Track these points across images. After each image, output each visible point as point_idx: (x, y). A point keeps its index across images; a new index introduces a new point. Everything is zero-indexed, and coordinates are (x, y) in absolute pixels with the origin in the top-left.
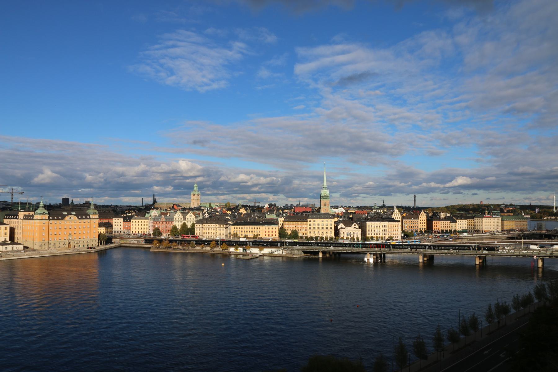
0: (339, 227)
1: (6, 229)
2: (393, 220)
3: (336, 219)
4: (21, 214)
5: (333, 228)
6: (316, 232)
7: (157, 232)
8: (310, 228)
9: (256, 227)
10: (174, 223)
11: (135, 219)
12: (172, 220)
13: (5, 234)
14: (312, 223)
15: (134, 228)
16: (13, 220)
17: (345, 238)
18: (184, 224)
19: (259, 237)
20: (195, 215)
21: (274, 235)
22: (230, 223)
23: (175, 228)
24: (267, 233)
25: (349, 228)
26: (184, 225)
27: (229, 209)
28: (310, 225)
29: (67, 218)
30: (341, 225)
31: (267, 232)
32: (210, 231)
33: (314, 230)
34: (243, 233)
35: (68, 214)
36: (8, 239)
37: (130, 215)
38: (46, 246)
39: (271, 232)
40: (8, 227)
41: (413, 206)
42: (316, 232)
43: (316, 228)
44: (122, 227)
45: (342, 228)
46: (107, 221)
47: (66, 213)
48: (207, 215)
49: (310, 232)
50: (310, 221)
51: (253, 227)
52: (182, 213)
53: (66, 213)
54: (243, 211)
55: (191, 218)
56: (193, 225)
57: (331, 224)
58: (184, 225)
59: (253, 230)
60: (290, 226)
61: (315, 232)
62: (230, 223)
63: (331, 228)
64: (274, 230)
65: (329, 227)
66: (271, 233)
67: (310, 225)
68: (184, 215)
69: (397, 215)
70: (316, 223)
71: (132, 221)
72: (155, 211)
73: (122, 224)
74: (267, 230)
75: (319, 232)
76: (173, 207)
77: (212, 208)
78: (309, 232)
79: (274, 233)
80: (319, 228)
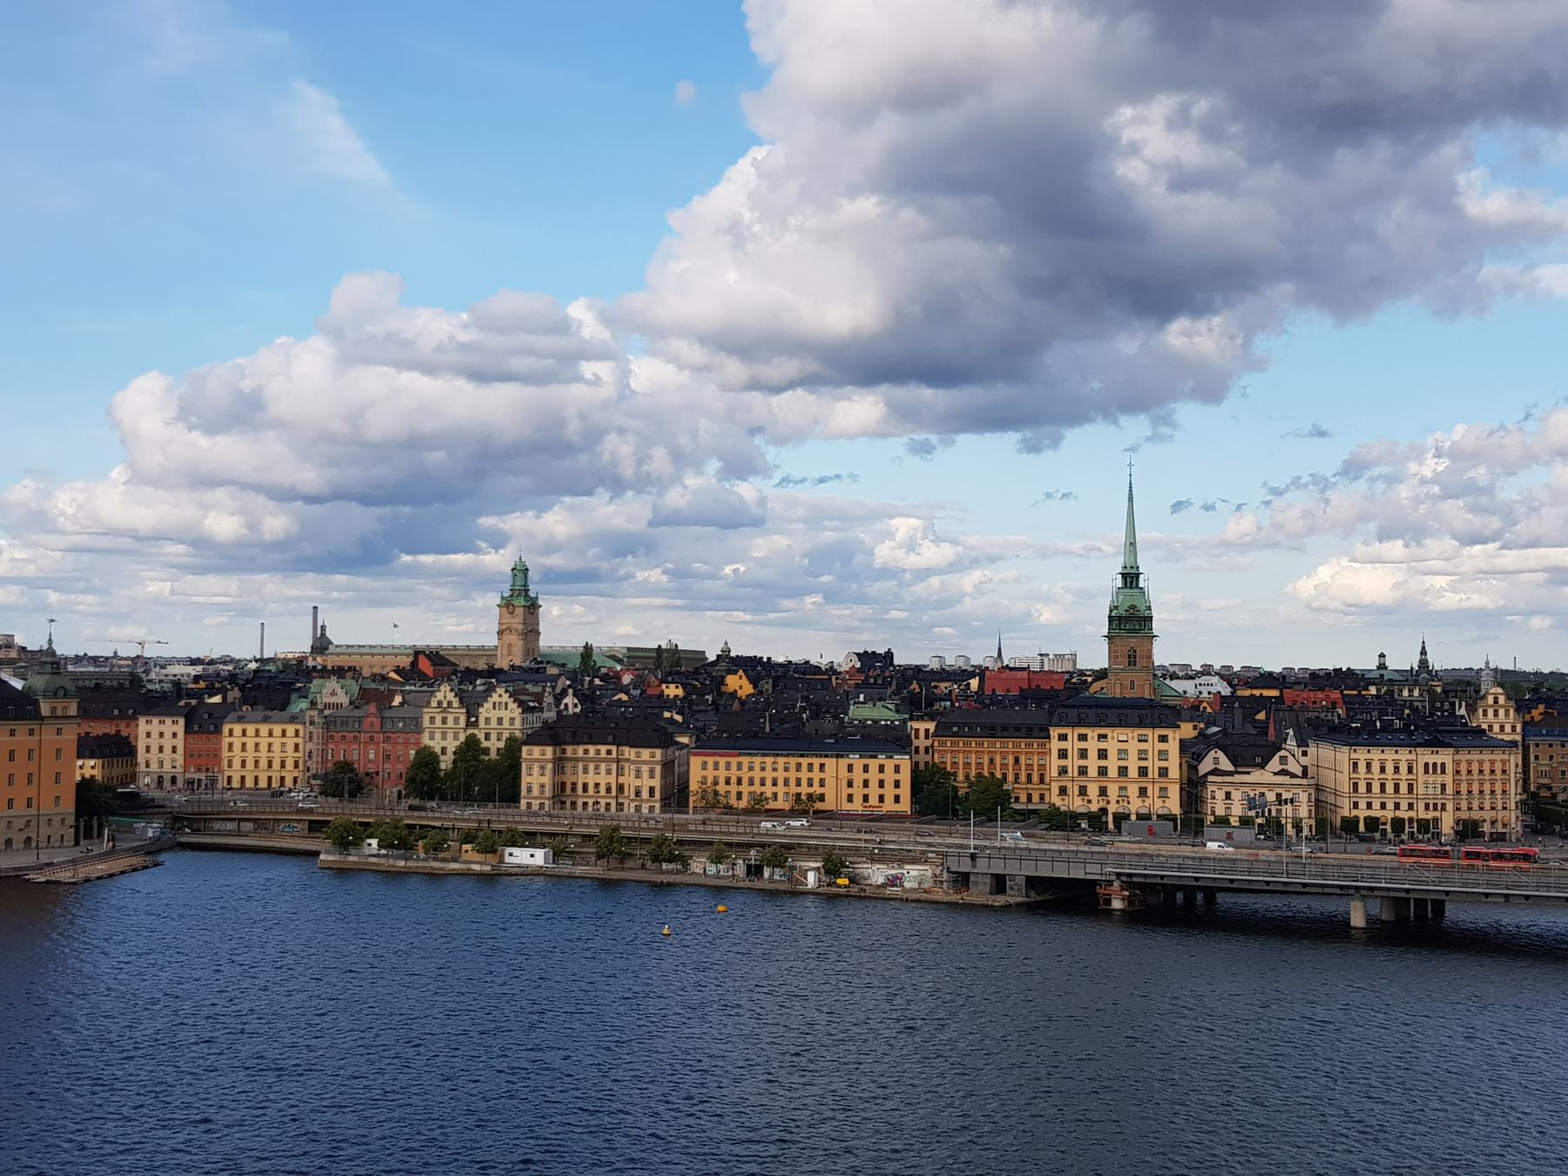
0: (1205, 766)
2: (1477, 738)
3: (1187, 730)
5: (1174, 773)
6: (1093, 791)
7: (343, 781)
8: (1063, 771)
9: (805, 761)
10: (426, 740)
11: (240, 720)
12: (415, 726)
14: (1073, 745)
15: (237, 764)
17: (1234, 821)
19: (819, 806)
20: (521, 704)
21: (889, 799)
22: (684, 740)
23: (427, 760)
24: (858, 792)
25: (1256, 776)
27: (670, 677)
28: (1063, 754)
30: (1217, 759)
31: (858, 782)
32: (591, 779)
33: (1082, 781)
34: (745, 788)
37: (217, 699)
39: (874, 784)
42: (1093, 791)
43: (1093, 772)
50: (1063, 737)
51: (793, 761)
52: (462, 696)
54: (738, 684)
55: (501, 716)
56: (512, 750)
57: (1163, 755)
58: (471, 748)
59: (792, 775)
60: (967, 759)
61: (1083, 791)
62: (684, 740)
63: (1163, 772)
65: (1153, 765)
66: (874, 792)
68: (471, 705)
69: (1499, 719)
70: (1093, 746)
71: (226, 728)
72: (332, 683)
73: (180, 742)
74: (858, 776)
75: (1103, 792)
76: (414, 664)
77: (595, 672)
79: (889, 792)
80: (1103, 771)
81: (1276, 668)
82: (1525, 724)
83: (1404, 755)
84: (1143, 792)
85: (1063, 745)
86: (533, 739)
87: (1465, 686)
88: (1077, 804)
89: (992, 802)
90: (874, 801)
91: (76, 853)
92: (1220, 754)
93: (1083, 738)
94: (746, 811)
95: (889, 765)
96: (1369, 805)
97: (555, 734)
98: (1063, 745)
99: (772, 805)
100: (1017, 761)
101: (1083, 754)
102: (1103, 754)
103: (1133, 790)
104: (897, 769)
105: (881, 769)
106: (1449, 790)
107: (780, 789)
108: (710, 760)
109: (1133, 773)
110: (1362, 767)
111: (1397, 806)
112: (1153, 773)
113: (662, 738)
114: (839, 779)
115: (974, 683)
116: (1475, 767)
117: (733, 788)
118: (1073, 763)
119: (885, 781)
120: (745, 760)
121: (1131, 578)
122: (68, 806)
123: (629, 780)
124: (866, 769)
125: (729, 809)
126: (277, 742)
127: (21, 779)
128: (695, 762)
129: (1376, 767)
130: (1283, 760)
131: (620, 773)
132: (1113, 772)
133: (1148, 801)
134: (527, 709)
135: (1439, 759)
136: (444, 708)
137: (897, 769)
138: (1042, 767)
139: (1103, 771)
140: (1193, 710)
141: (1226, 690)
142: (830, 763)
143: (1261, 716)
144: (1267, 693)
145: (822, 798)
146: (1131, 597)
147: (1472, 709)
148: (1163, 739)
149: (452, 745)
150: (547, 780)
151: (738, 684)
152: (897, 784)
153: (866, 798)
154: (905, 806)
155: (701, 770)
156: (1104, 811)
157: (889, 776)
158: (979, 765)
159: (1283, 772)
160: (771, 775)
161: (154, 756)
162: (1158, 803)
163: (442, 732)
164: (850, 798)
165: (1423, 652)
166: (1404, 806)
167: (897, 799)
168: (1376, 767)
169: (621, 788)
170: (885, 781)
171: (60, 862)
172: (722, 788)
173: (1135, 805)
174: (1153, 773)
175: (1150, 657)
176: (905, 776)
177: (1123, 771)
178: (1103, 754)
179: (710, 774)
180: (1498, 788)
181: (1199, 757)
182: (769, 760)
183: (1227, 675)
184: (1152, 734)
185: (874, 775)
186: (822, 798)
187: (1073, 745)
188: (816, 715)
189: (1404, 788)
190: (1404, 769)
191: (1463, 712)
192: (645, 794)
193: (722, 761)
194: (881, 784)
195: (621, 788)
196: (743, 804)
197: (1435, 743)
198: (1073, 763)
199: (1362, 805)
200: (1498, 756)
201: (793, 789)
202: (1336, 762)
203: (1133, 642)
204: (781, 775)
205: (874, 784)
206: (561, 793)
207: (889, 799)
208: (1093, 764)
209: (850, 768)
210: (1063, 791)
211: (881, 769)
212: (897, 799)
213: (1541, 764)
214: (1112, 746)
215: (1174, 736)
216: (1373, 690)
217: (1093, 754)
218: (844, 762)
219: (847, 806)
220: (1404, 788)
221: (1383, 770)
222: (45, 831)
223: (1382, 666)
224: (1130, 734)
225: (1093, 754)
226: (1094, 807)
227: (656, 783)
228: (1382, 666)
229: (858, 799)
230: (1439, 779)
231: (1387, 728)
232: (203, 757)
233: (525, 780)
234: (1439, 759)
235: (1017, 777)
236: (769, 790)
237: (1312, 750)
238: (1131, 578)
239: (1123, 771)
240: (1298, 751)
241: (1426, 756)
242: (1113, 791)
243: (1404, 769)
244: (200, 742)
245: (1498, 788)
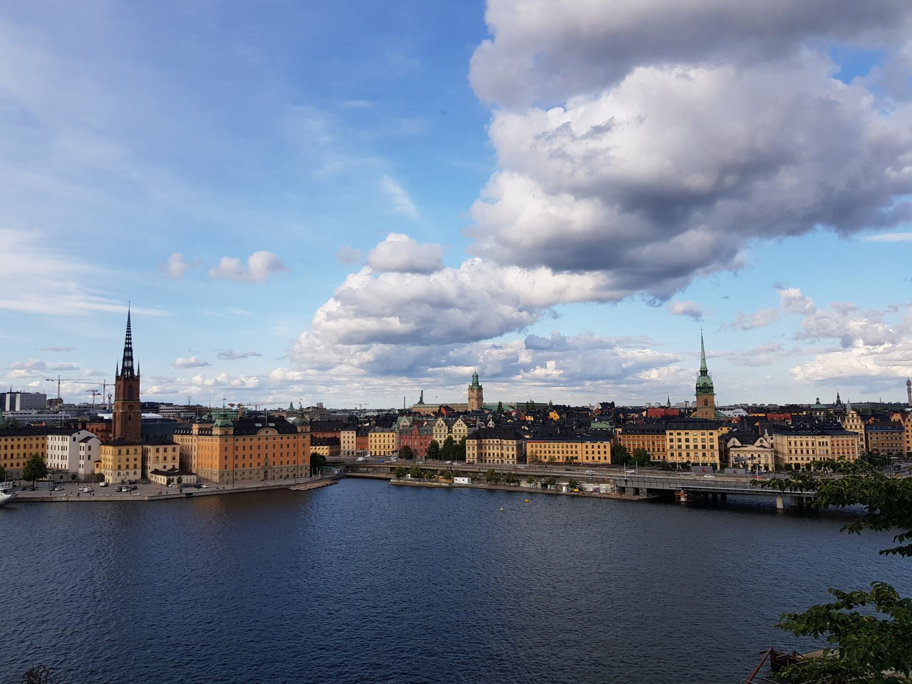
0: (730, 444)
1: (174, 450)
3: (725, 430)
4: (195, 428)
5: (716, 447)
6: (684, 454)
7: (407, 453)
8: (672, 447)
9: (569, 444)
10: (435, 438)
13: (174, 459)
14: (675, 437)
16: (185, 437)
18: (450, 438)
19: (575, 461)
20: (467, 424)
21: (602, 458)
22: (528, 437)
23: (435, 445)
24: (590, 456)
25: (750, 447)
26: (450, 441)
28: (671, 440)
29: (262, 433)
30: (735, 441)
32: (491, 451)
35: (263, 427)
36: (177, 466)
38: (230, 478)
39: (596, 453)
40: (178, 448)
41: (907, 401)
42: (684, 454)
43: (684, 447)
44: (354, 445)
45: (734, 446)
46: (330, 435)
47: (260, 425)
48: (491, 424)
49: (672, 455)
50: (671, 434)
51: (565, 444)
52: (446, 421)
53: (260, 425)
57: (712, 440)
58: (450, 441)
59: (565, 449)
60: (632, 443)
61: (680, 455)
62: (528, 437)
63: (712, 447)
64: (602, 450)
66: (596, 456)
67: (671, 440)
68: (450, 425)
69: (854, 424)
70: (683, 437)
73: (354, 440)
74: (590, 450)
75: (688, 455)
78: (669, 454)
79: (602, 455)
80: (688, 447)
81: (782, 403)
82: (866, 425)
83: (810, 439)
84: (704, 455)
85: (671, 437)
86: (470, 437)
87: (839, 410)
88: (677, 459)
89: (643, 460)
90: (596, 459)
91: (309, 480)
92: (736, 440)
93: (679, 434)
94: (548, 463)
95: (602, 445)
96: (797, 459)
97: (478, 435)
98: (671, 437)
99: (557, 461)
100: (653, 443)
101: (680, 440)
102: (687, 440)
103: (700, 454)
104: (605, 447)
105: (599, 447)
106: (830, 452)
107: (561, 455)
108: (534, 444)
109: (700, 447)
110: (793, 443)
111: (797, 459)
112: (708, 447)
113: (518, 436)
114: (583, 451)
115: (644, 414)
116: (840, 443)
117: (543, 455)
118: (676, 444)
119: (602, 451)
120: (547, 444)
121: (704, 372)
122: (308, 463)
123: (505, 452)
124: (593, 447)
125: (541, 462)
126: (386, 439)
127: (291, 454)
128: (529, 445)
129: (798, 444)
130: (761, 441)
131: (502, 449)
132: (692, 447)
133: (707, 459)
134: (469, 426)
135: (825, 440)
136: (440, 426)
137: (605, 447)
138: (663, 446)
139: (688, 447)
140: (728, 422)
141: (744, 414)
142: (579, 445)
143: (757, 424)
144: (760, 415)
145: (576, 458)
146: (704, 380)
147: (843, 420)
148: (711, 434)
149: (443, 439)
150: (475, 452)
151: (554, 415)
152: (605, 453)
153: (593, 458)
154: (609, 461)
155: (531, 448)
156: (689, 462)
157: (602, 450)
158: (639, 445)
159: (762, 446)
160: (557, 450)
161: (346, 445)
162: (711, 459)
163: (440, 435)
164: (587, 458)
165: (838, 397)
166: (800, 458)
167: (605, 458)
168: (798, 444)
169: (502, 454)
170: (602, 451)
171: (304, 483)
172: (538, 454)
173: (701, 460)
174: (708, 447)
175: (713, 402)
176: (608, 450)
177: (696, 447)
178: (687, 440)
179: (534, 449)
180: (851, 451)
181: (727, 441)
182: (556, 444)
183: (747, 409)
184: (707, 432)
185: (596, 449)
186: (576, 458)
187: (675, 437)
188: (579, 427)
189: (811, 452)
190: (810, 444)
191: (839, 421)
192: (511, 457)
193: (538, 444)
194: (593, 453)
195: (502, 454)
196: (546, 461)
197: (823, 434)
198: (676, 444)
199: (794, 458)
200: (850, 438)
201: (566, 455)
202: (783, 442)
203: (706, 397)
204: (560, 450)
205: (596, 453)
206: (481, 457)
207: (602, 458)
208: (684, 444)
209: (587, 447)
210: (672, 455)
211: (599, 447)
212: (605, 458)
213: (873, 441)
214: (691, 437)
215: (716, 434)
216: (805, 413)
217: (683, 440)
218: (584, 445)
219: (585, 461)
220: (811, 452)
221: (801, 445)
222: (300, 472)
223: (818, 403)
224: (699, 432)
225: (683, 440)
226: (685, 461)
227: (515, 453)
228: (818, 403)
229: (590, 458)
230: (825, 448)
231: (805, 428)
232: (362, 446)
233: (467, 452)
234: (825, 440)
235: (654, 450)
236: (556, 455)
237: (774, 437)
238: (704, 372)
239: (696, 447)
240: (769, 438)
241: (819, 439)
242: (692, 454)
243: (810, 444)
244: (361, 440)
245: (851, 451)
